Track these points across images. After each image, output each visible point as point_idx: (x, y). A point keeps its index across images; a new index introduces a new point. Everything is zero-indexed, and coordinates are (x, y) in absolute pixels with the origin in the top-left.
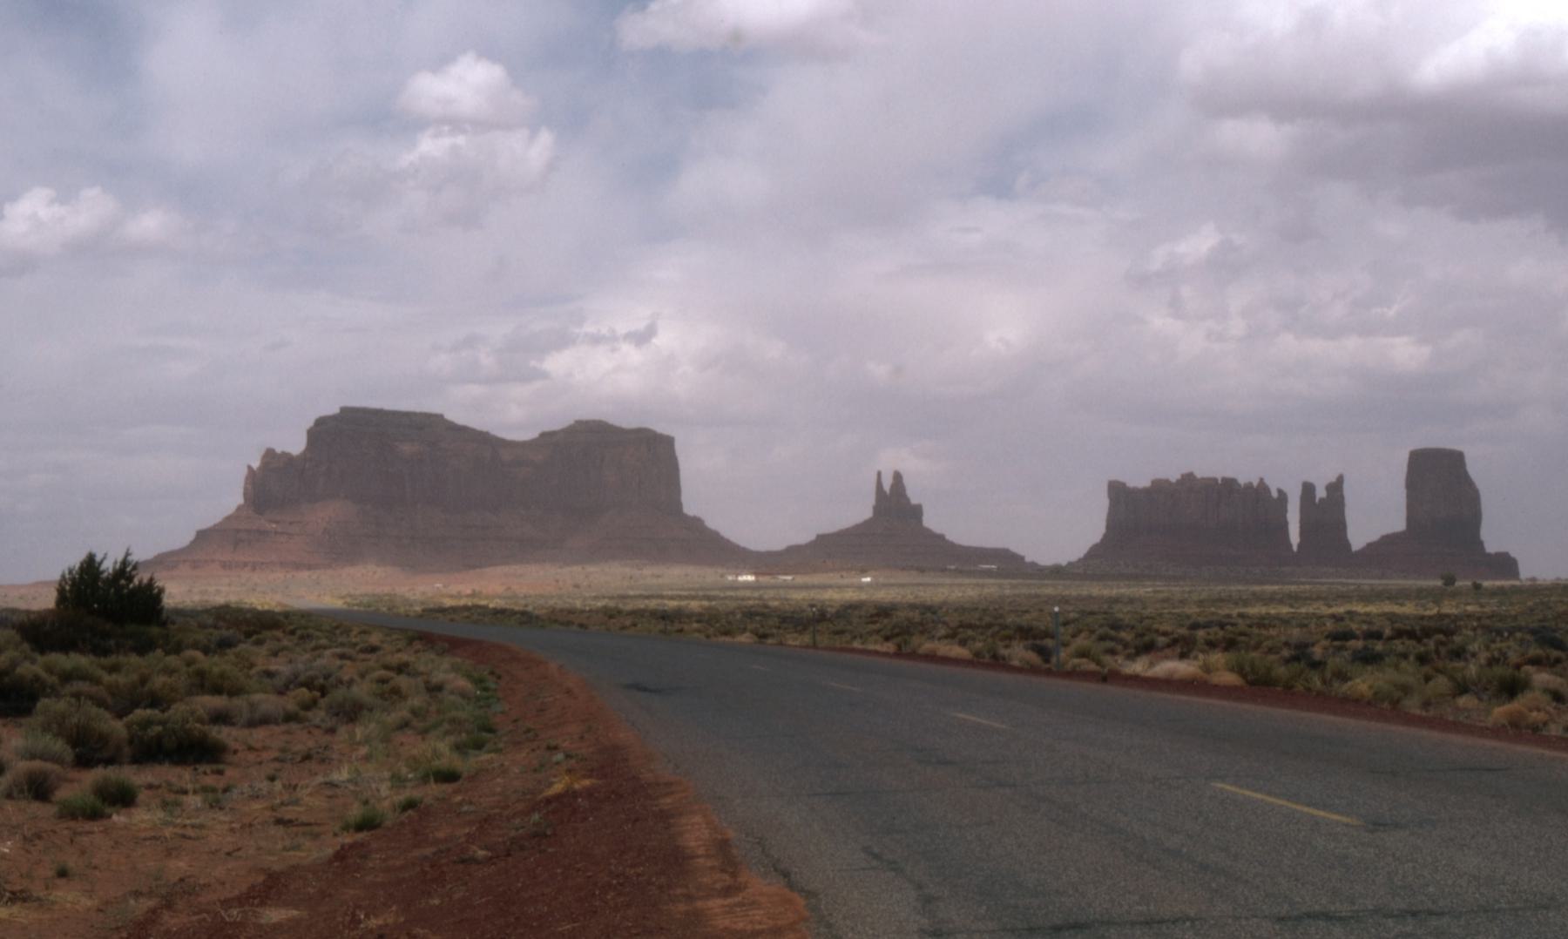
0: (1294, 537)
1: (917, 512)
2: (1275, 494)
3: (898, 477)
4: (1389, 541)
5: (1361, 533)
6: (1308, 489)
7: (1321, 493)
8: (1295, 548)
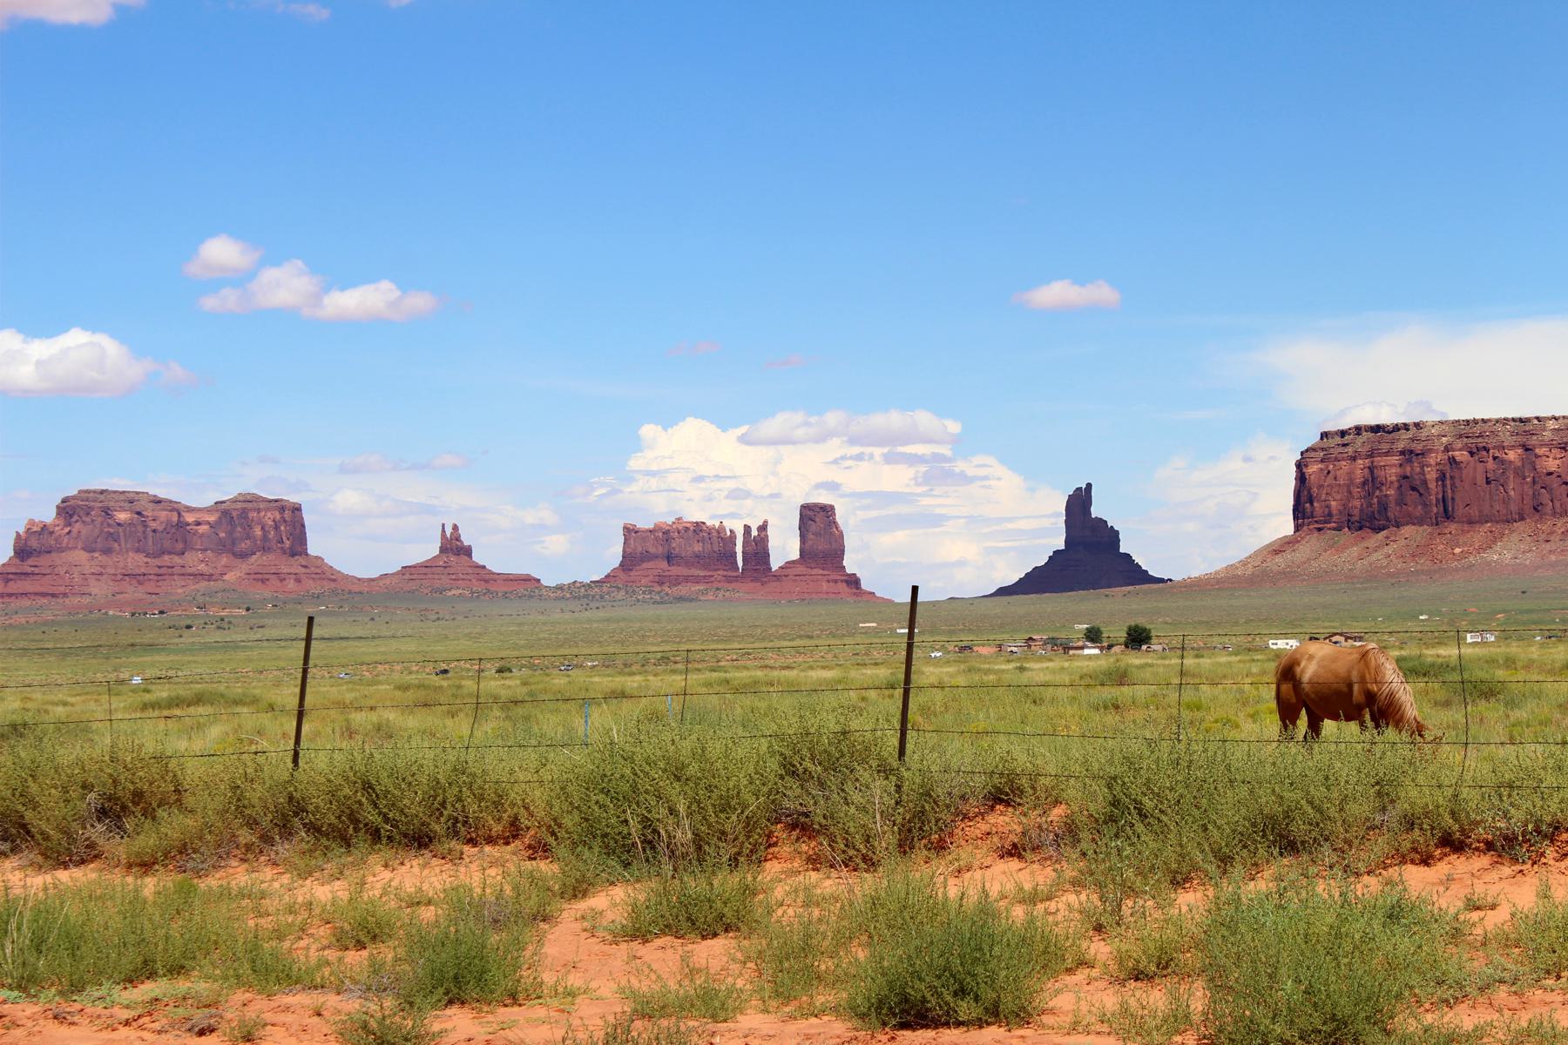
1: (468, 551)
2: (729, 533)
3: (455, 528)
4: (790, 564)
5: (776, 563)
6: (747, 529)
7: (754, 533)
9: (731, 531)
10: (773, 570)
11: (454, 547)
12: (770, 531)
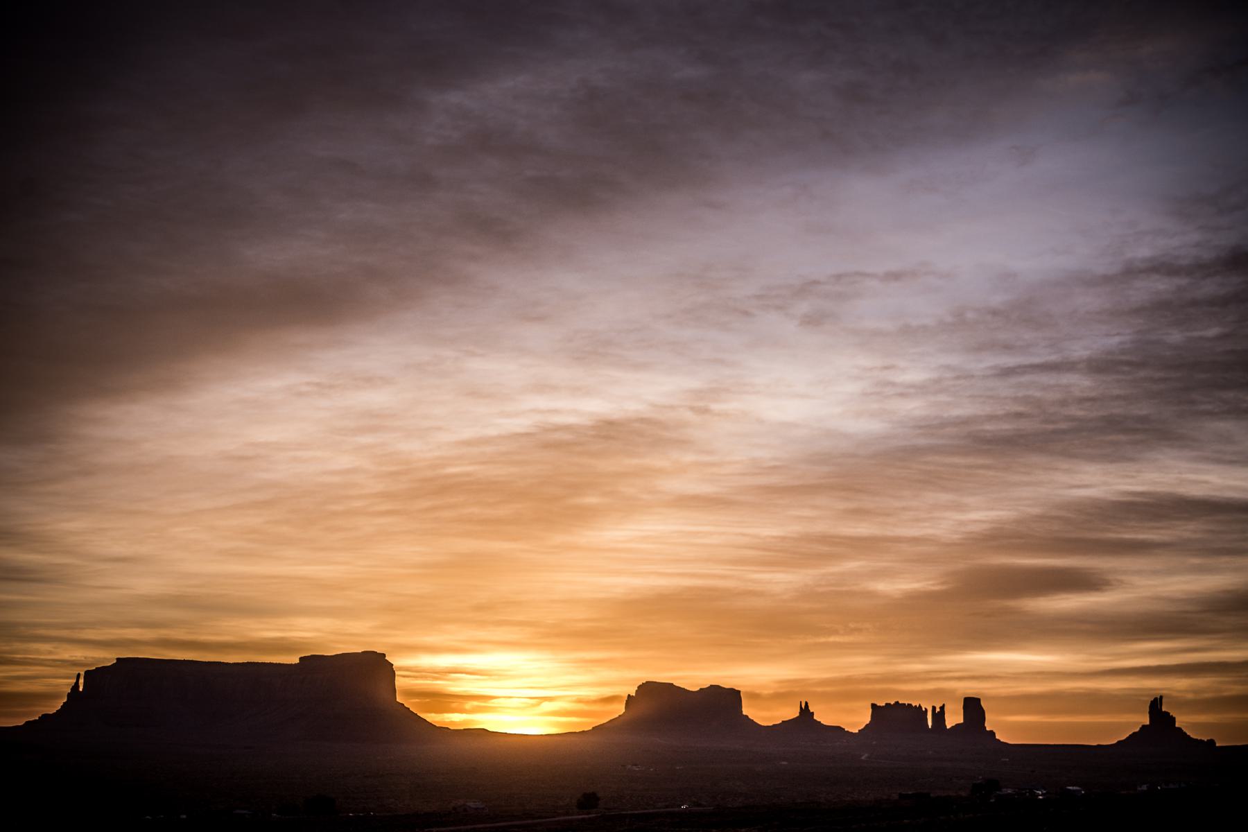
0: (930, 724)
2: (924, 709)
3: (806, 703)
6: (934, 708)
7: (938, 710)
8: (930, 727)
9: (926, 709)
10: (948, 727)
11: (805, 712)
12: (946, 709)
